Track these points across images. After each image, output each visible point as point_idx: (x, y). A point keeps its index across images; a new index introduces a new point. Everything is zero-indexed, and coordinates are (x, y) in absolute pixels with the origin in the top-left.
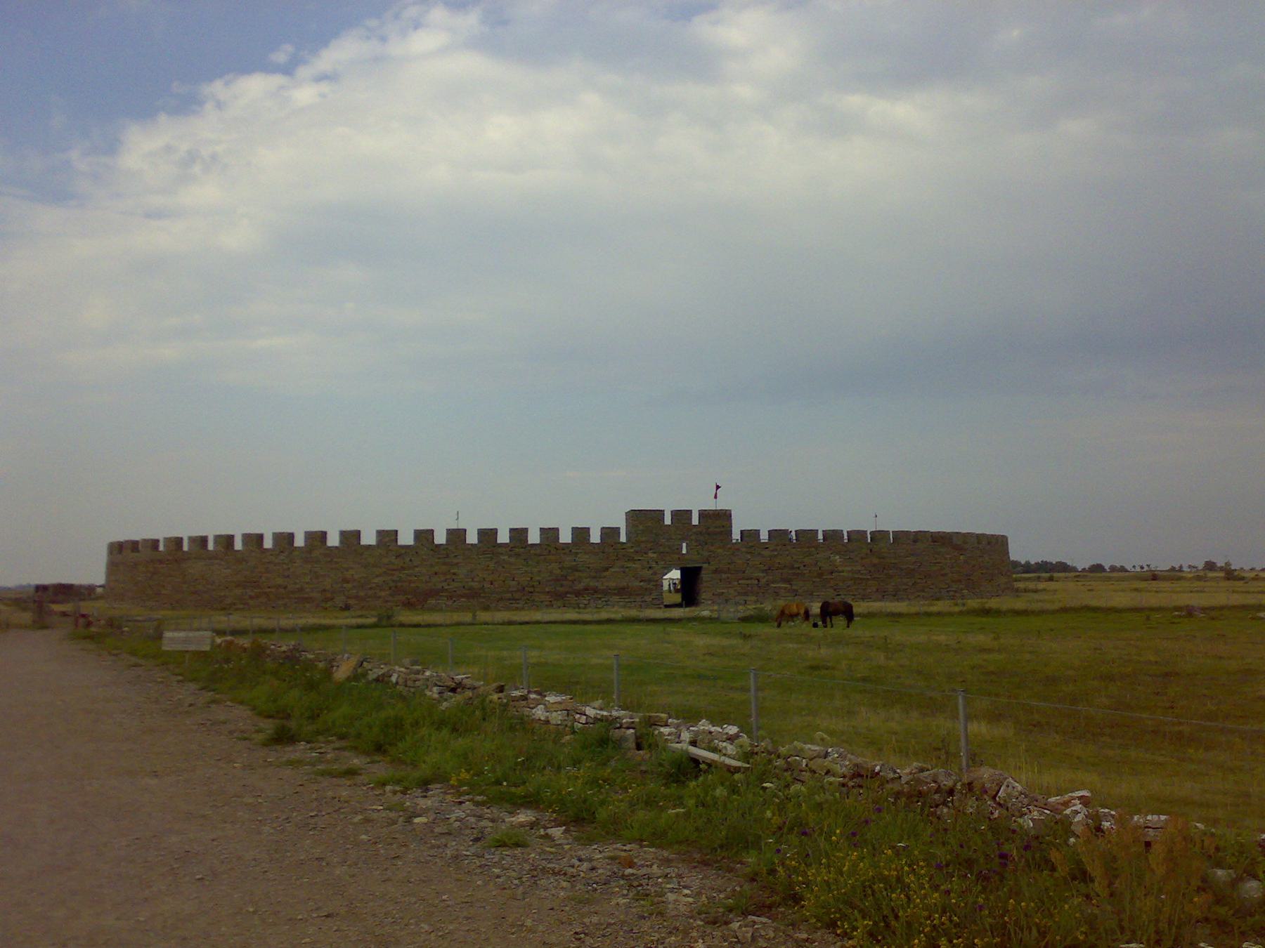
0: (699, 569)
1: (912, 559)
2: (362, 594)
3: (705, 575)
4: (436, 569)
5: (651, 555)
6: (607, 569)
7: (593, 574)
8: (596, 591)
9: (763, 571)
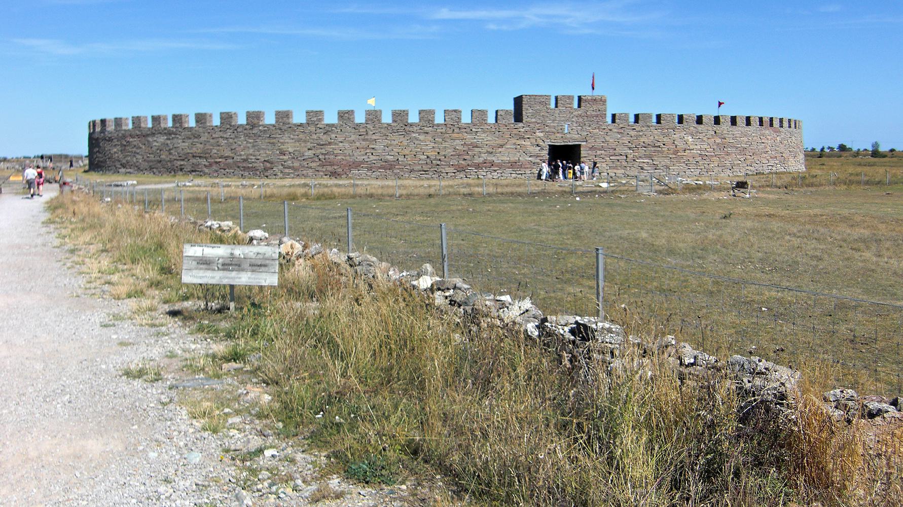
1: (745, 139)
2: (296, 164)
4: (358, 144)
5: (539, 134)
6: (502, 146)
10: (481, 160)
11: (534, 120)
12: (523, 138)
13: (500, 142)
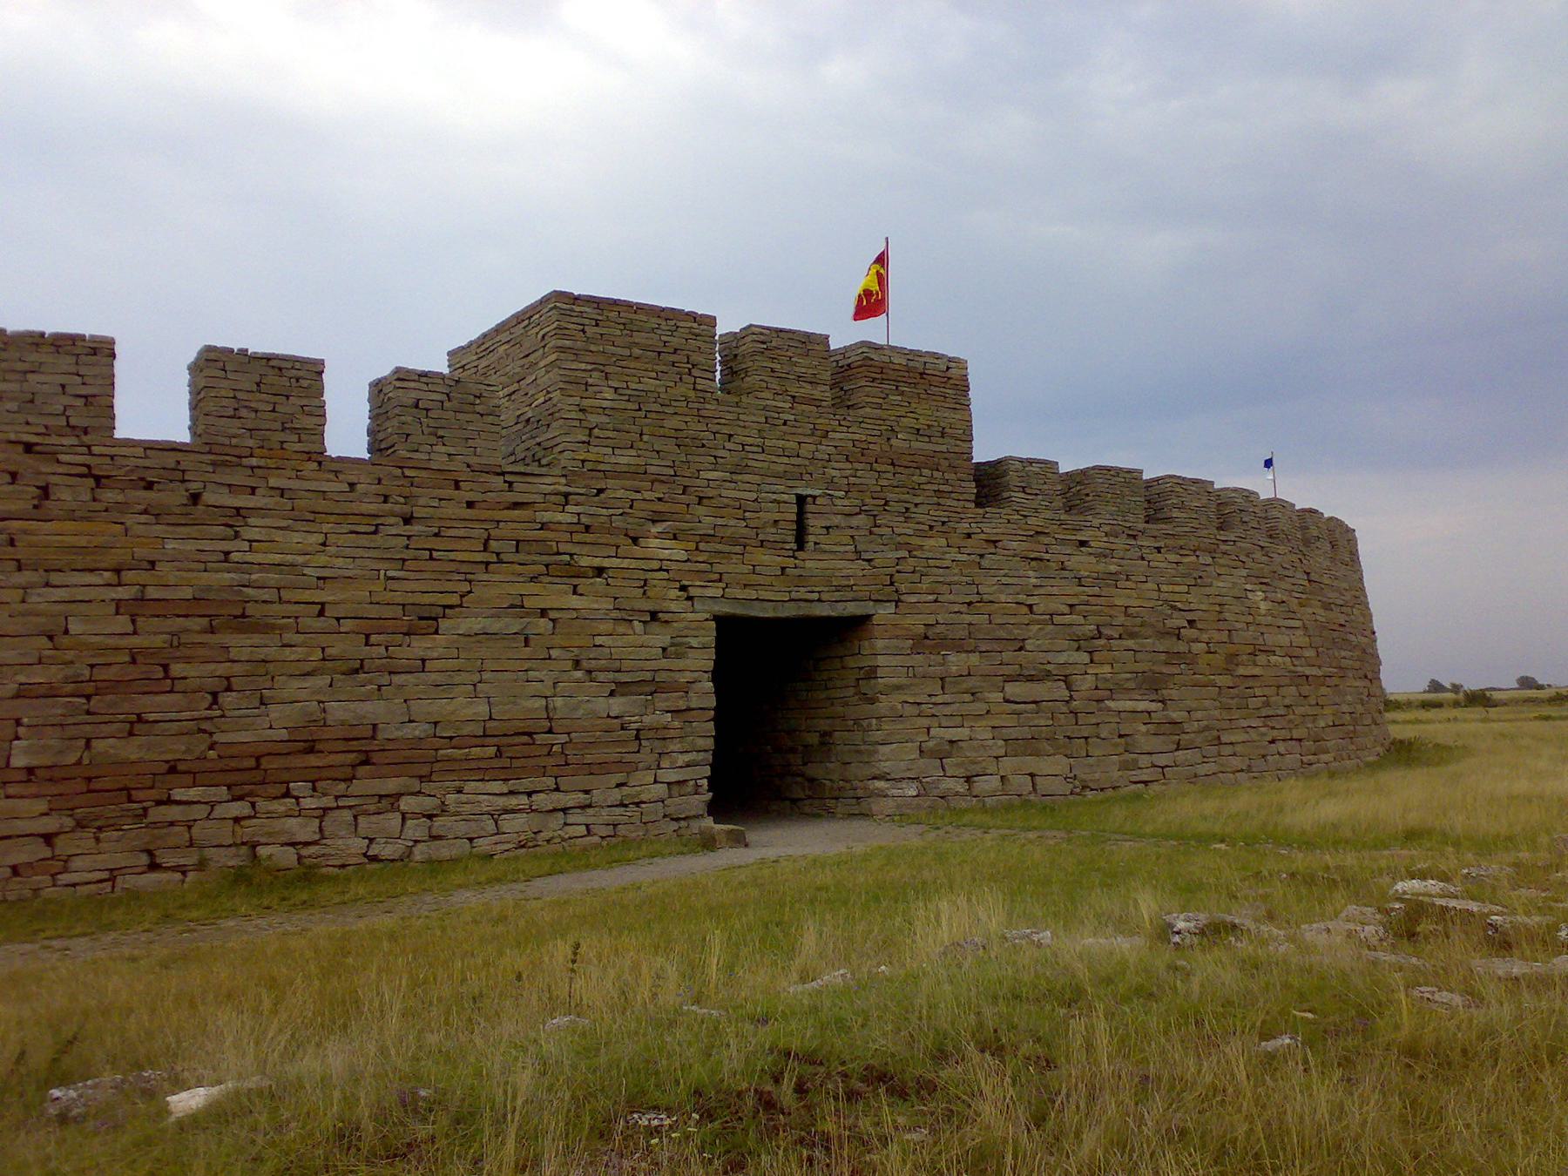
0: (857, 625)
3: (884, 654)
5: (658, 547)
6: (428, 620)
7: (346, 647)
8: (365, 751)
9: (1079, 642)
10: (276, 723)
11: (625, 459)
12: (572, 573)
13: (421, 589)
